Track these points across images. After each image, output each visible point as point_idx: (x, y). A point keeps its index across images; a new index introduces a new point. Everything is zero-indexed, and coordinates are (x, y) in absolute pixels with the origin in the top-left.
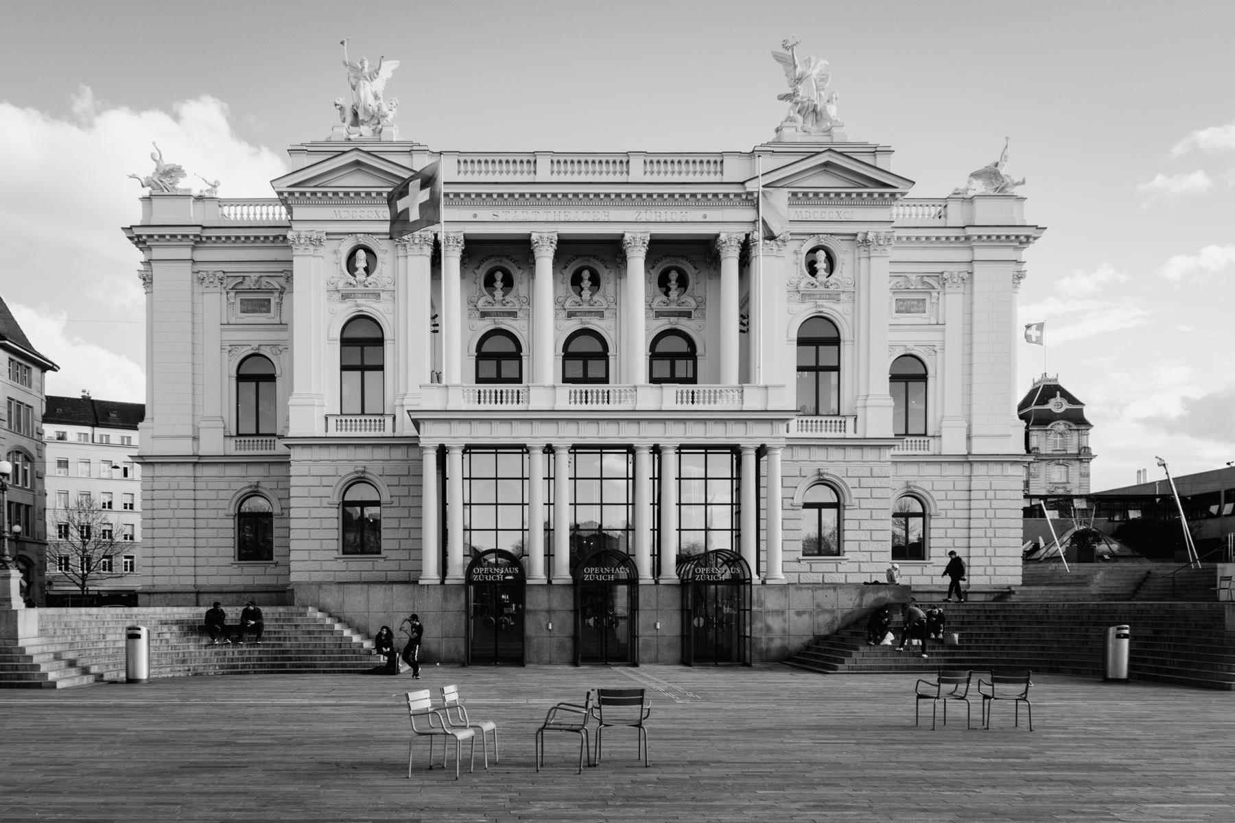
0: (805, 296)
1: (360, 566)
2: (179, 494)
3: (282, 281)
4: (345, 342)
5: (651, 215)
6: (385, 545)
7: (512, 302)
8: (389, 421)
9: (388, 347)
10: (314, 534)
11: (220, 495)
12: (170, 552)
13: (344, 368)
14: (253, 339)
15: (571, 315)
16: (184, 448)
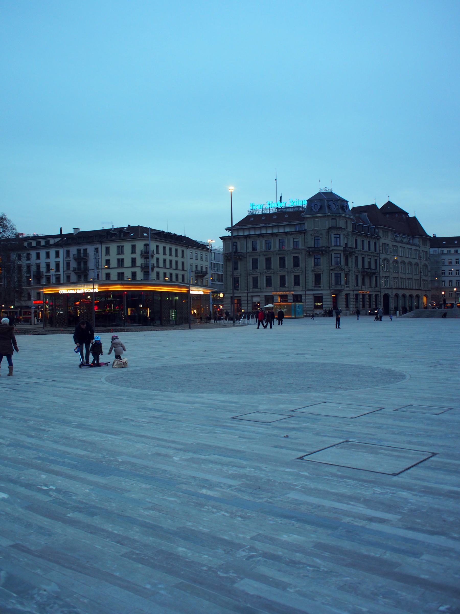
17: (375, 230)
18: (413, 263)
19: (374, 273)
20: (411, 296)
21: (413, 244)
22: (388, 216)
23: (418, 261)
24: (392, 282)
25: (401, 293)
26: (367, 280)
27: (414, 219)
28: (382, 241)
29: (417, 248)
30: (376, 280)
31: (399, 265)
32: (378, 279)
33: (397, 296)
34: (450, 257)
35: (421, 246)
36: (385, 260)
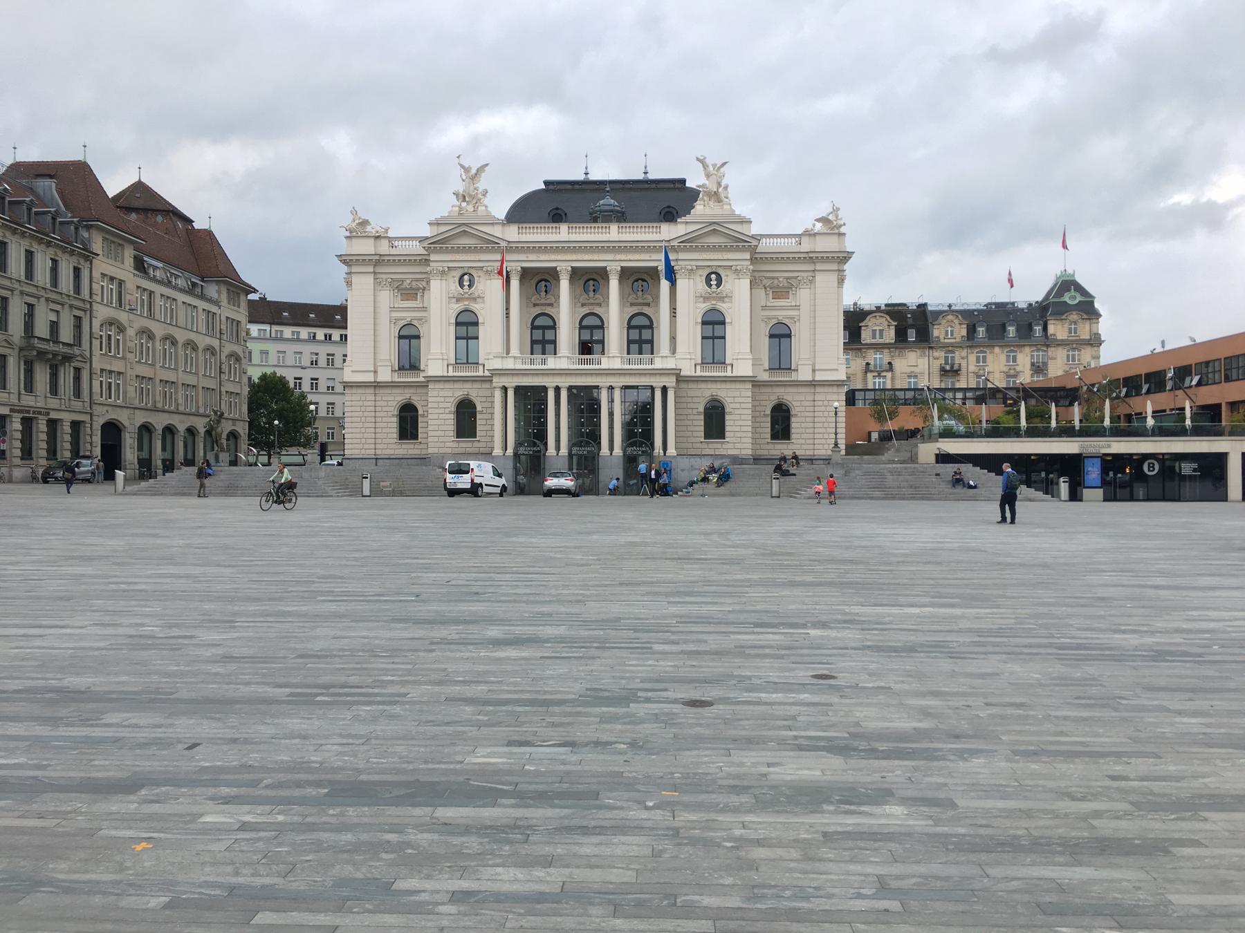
0: (706, 299)
1: (466, 444)
3: (424, 284)
4: (458, 324)
5: (623, 257)
8: (481, 368)
9: (480, 327)
10: (442, 428)
11: (391, 404)
13: (457, 338)
14: (408, 316)
15: (583, 305)
16: (369, 378)
17: (76, 229)
18: (201, 346)
19: (67, 358)
20: (191, 431)
21: (202, 297)
22: (134, 216)
23: (216, 343)
24: (131, 390)
25: (159, 422)
26: (42, 376)
27: (209, 234)
28: (102, 265)
29: (214, 309)
30: (77, 379)
31: (159, 346)
32: (85, 375)
33: (146, 429)
36: (111, 324)
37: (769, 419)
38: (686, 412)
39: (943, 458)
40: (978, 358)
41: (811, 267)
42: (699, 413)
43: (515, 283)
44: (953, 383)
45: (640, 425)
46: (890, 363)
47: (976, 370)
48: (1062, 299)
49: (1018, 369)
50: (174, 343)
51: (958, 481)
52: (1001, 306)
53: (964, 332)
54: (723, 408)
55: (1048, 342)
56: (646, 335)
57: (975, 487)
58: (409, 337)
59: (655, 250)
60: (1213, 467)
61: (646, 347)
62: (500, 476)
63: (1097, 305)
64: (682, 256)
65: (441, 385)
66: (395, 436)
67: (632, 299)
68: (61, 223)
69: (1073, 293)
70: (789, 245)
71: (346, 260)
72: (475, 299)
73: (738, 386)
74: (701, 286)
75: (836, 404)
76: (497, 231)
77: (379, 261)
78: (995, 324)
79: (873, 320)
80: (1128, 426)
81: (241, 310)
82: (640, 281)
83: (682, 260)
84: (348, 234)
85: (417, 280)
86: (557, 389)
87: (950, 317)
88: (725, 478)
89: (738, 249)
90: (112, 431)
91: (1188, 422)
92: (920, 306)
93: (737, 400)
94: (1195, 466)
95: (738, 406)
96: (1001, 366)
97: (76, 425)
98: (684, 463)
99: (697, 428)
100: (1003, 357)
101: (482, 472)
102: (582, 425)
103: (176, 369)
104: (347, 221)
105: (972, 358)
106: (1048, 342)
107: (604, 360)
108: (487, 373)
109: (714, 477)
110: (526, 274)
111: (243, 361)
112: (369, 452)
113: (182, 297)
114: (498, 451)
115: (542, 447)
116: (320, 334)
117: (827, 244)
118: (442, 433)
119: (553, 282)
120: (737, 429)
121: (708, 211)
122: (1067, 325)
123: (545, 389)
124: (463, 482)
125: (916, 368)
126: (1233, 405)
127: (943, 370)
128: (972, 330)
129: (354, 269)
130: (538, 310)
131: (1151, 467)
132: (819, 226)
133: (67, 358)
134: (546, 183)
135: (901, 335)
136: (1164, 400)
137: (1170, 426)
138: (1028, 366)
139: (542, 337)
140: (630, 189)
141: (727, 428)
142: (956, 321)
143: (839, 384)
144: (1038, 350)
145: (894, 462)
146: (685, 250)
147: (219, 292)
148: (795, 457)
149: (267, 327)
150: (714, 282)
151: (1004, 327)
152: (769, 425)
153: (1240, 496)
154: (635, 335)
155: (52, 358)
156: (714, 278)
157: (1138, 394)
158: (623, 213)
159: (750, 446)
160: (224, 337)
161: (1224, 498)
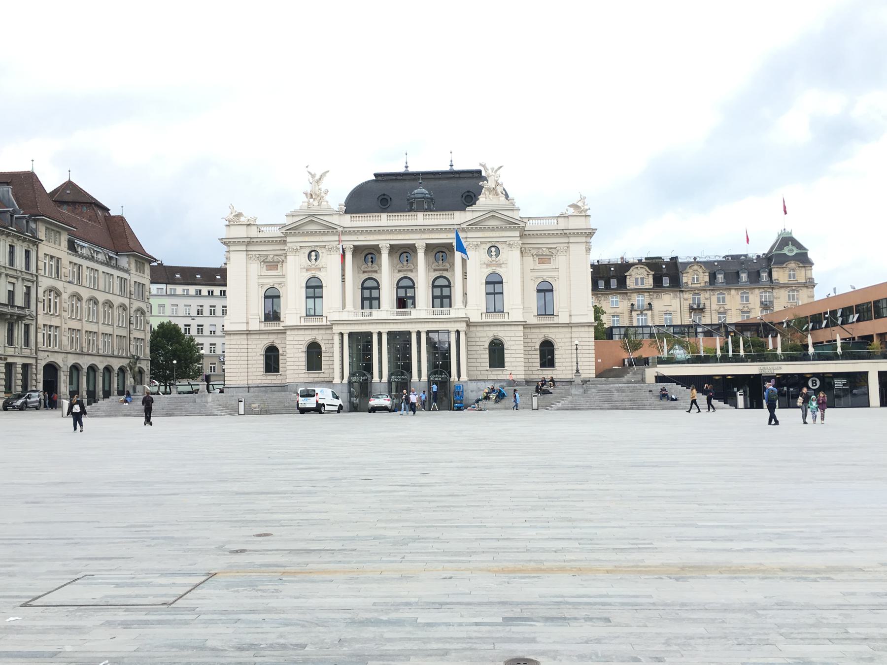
0: (488, 265)
1: (314, 375)
2: (241, 346)
3: (283, 258)
4: (307, 287)
6: (323, 367)
7: (376, 267)
8: (325, 319)
10: (296, 363)
12: (237, 370)
13: (307, 298)
14: (271, 282)
15: (399, 271)
16: (243, 327)
17: (27, 222)
18: (116, 304)
19: (21, 318)
20: (108, 369)
21: (117, 267)
23: (126, 301)
24: (65, 341)
25: (85, 362)
27: (121, 219)
29: (125, 275)
31: (85, 306)
33: (75, 368)
34: (188, 301)
35: (133, 271)
36: (51, 291)
37: (538, 352)
38: (475, 348)
39: (660, 379)
40: (719, 299)
41: (566, 240)
42: (485, 349)
43: (349, 257)
44: (700, 319)
45: (440, 360)
46: (650, 304)
47: (717, 308)
48: (783, 252)
49: (750, 306)
50: (96, 302)
51: (664, 396)
52: (736, 258)
53: (707, 279)
54: (502, 344)
55: (772, 285)
56: (446, 292)
57: (676, 400)
58: (272, 296)
59: (450, 231)
60: (858, 380)
61: (446, 301)
62: (337, 398)
63: (810, 255)
64: (470, 235)
65: (296, 332)
66: (263, 370)
67: (434, 266)
68: (16, 218)
69: (790, 247)
70: (551, 225)
71: (226, 242)
72: (320, 269)
73: (513, 328)
74: (485, 257)
75: (577, 342)
76: (335, 220)
77: (250, 242)
78: (731, 272)
79: (636, 270)
80: (798, 353)
81: (146, 275)
82: (440, 253)
83: (468, 239)
84: (227, 223)
85: (277, 255)
86: (380, 334)
87: (695, 267)
88: (501, 396)
89: (510, 229)
90: (51, 370)
91: (839, 350)
92: (672, 259)
93: (513, 339)
94: (845, 381)
95: (513, 343)
96: (737, 306)
97: (25, 367)
98: (473, 386)
99: (483, 360)
100: (738, 298)
101: (324, 395)
102: (398, 359)
103: (97, 323)
104: (227, 214)
105: (714, 298)
106: (772, 285)
107: (413, 311)
108: (329, 323)
109: (493, 396)
110: (357, 250)
111: (147, 314)
112: (243, 382)
113: (102, 268)
114: (337, 380)
115: (369, 376)
116: (205, 290)
117: (576, 224)
118: (296, 368)
119: (377, 255)
120: (514, 360)
121: (489, 202)
122: (787, 272)
123: (370, 334)
124: (311, 403)
125: (670, 308)
126: (881, 335)
127: (691, 309)
128: (713, 277)
129: (232, 248)
130: (366, 276)
131: (814, 383)
132: (571, 211)
133: (21, 318)
134: (375, 175)
135: (658, 282)
136: (824, 335)
137: (826, 353)
138: (759, 304)
139: (369, 296)
140: (440, 178)
141: (506, 360)
142: (701, 270)
143: (588, 325)
144: (766, 292)
145: (630, 382)
146: (472, 230)
147: (129, 263)
148: (552, 380)
149: (163, 286)
150: (493, 254)
151: (737, 274)
152: (538, 356)
153: (878, 404)
154: (437, 292)
155: (12, 318)
156: (494, 250)
157: (820, 328)
158: (432, 199)
159: (523, 372)
160: (133, 297)
161: (867, 405)
